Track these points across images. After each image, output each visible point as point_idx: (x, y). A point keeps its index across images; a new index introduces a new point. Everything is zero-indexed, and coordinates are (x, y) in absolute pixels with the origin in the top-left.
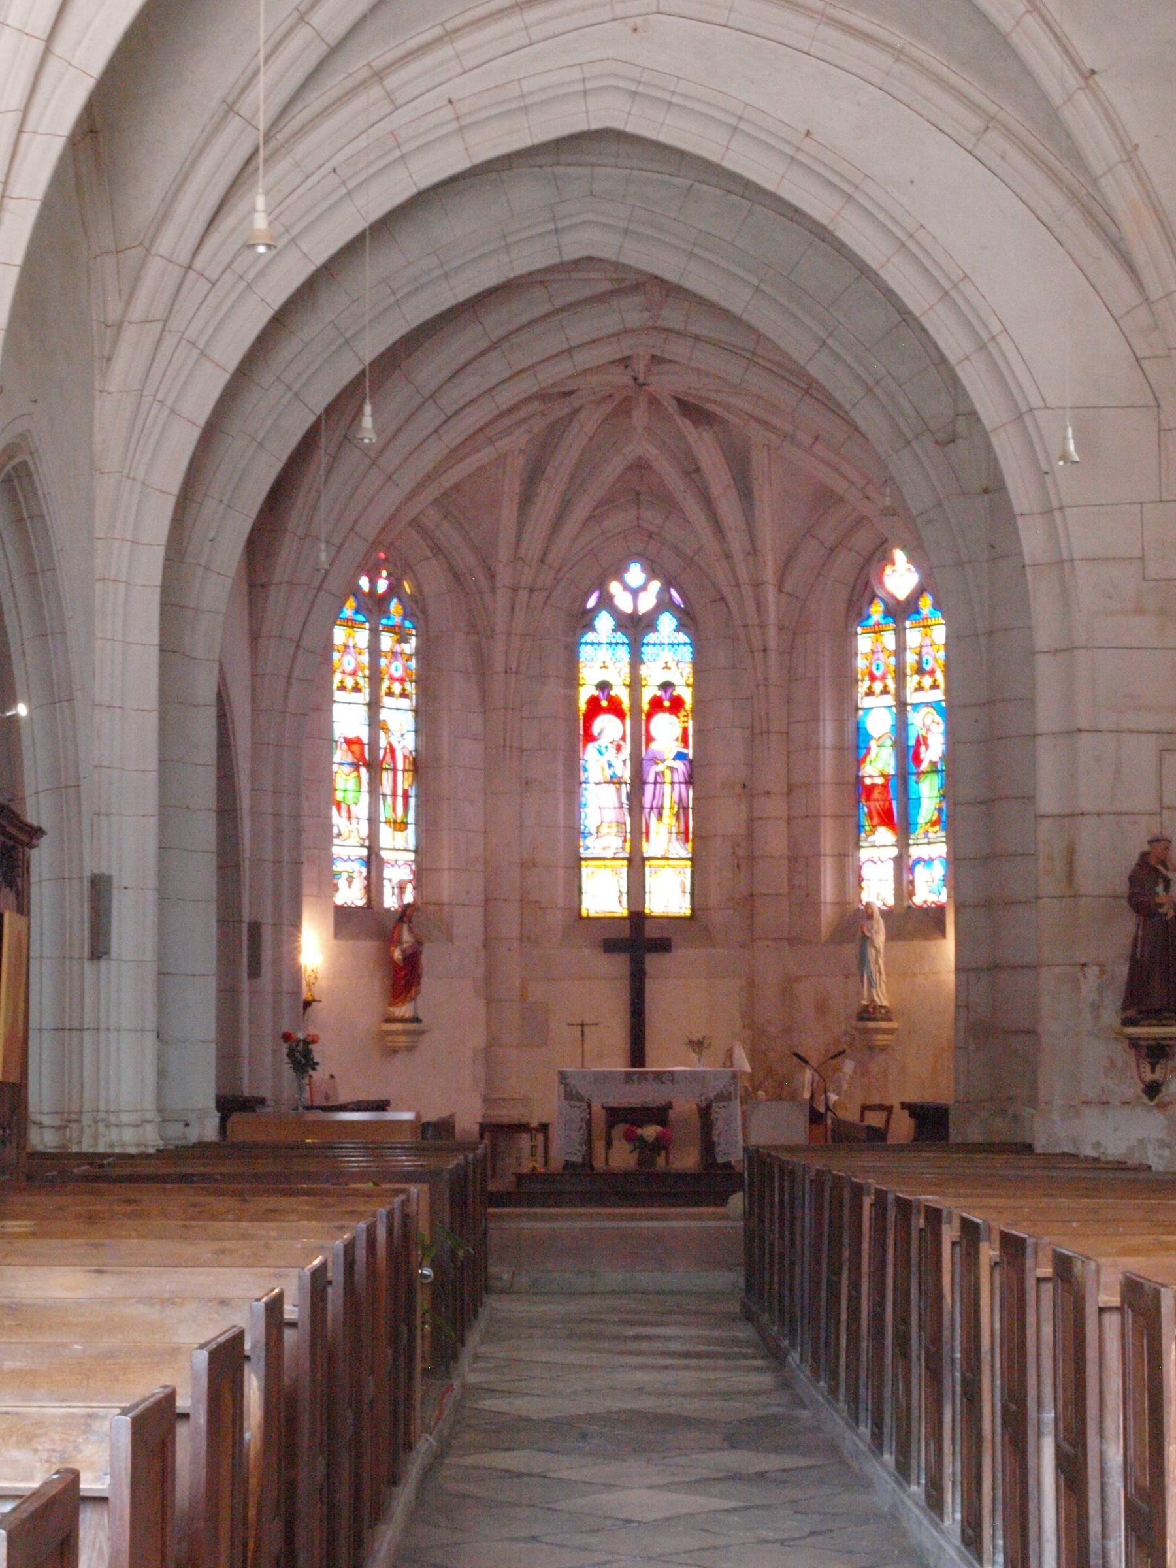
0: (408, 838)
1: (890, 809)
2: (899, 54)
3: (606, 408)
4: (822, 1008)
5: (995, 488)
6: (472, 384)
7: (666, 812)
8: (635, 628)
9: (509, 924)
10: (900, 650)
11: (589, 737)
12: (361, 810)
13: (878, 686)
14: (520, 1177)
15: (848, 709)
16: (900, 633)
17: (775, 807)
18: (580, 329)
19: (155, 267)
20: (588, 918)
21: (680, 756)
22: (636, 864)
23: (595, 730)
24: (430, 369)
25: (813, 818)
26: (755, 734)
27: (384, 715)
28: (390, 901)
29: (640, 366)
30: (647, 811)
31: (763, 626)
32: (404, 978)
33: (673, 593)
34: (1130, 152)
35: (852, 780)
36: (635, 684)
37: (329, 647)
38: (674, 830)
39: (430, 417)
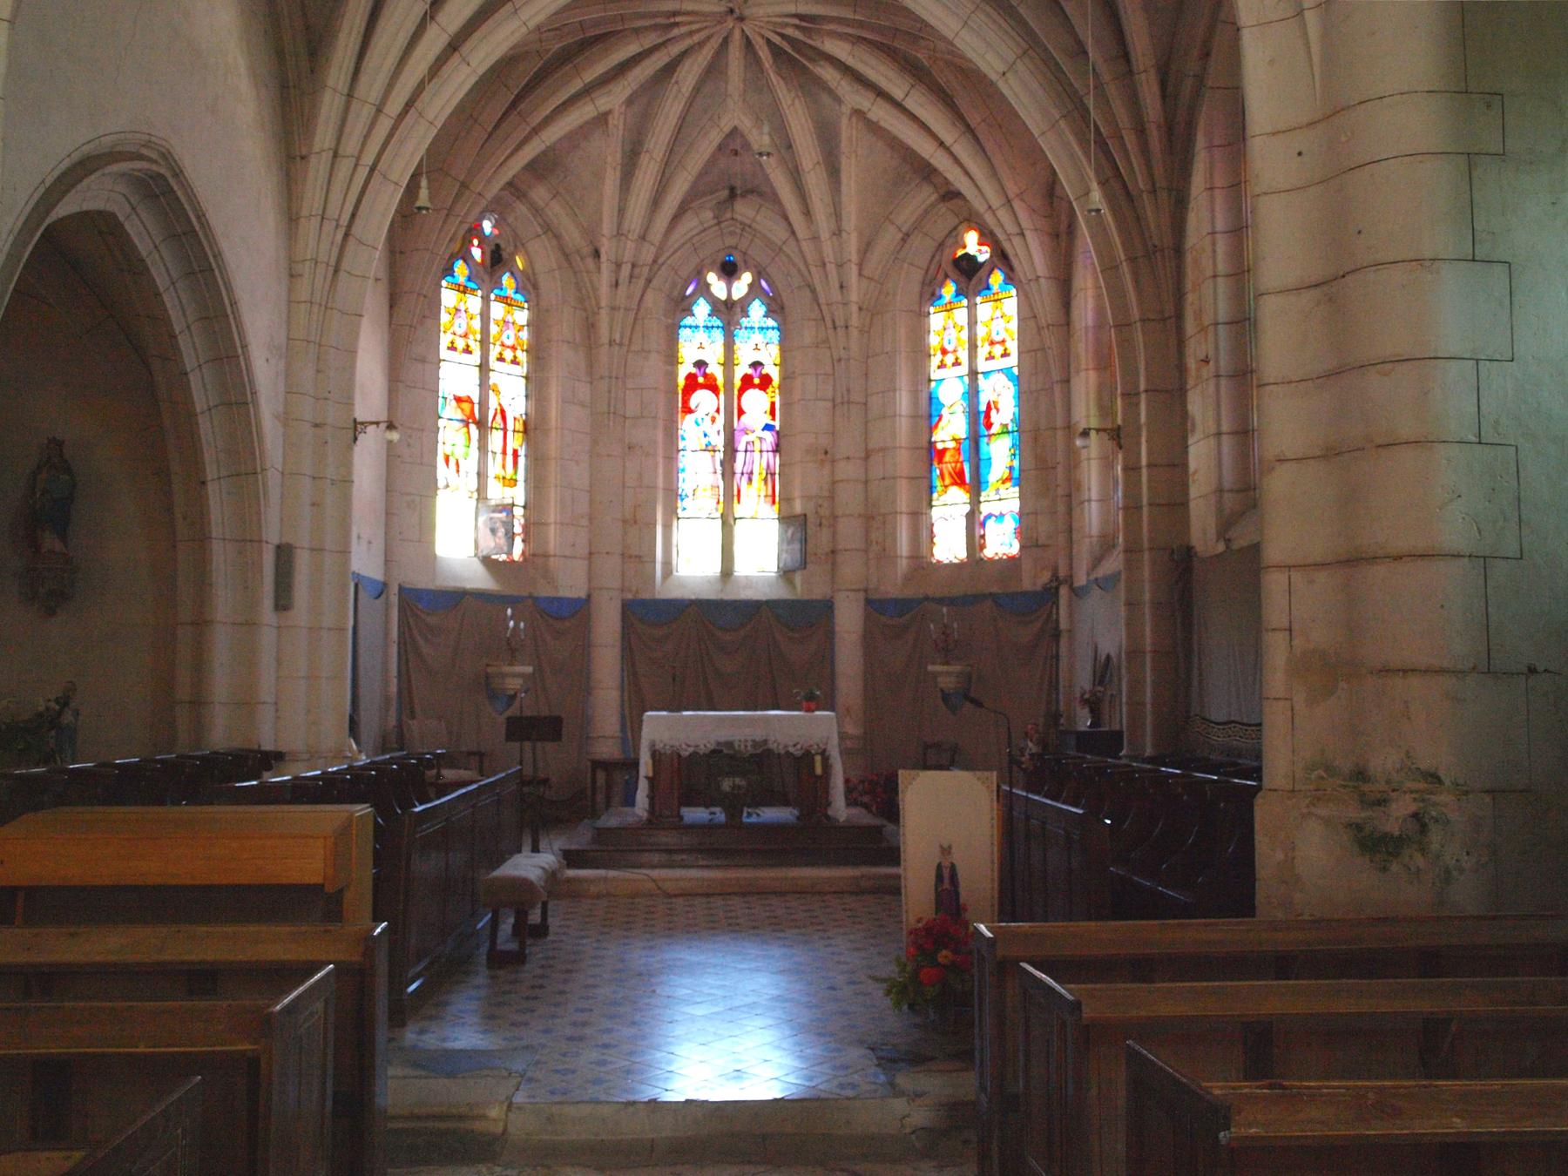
1: (961, 474)
7: (755, 477)
8: (729, 313)
10: (972, 322)
11: (688, 410)
12: (470, 465)
13: (949, 359)
16: (972, 308)
21: (768, 427)
23: (692, 404)
26: (837, 404)
27: (494, 378)
30: (738, 476)
33: (764, 283)
35: (925, 444)
36: (729, 363)
37: (433, 305)
38: (763, 493)
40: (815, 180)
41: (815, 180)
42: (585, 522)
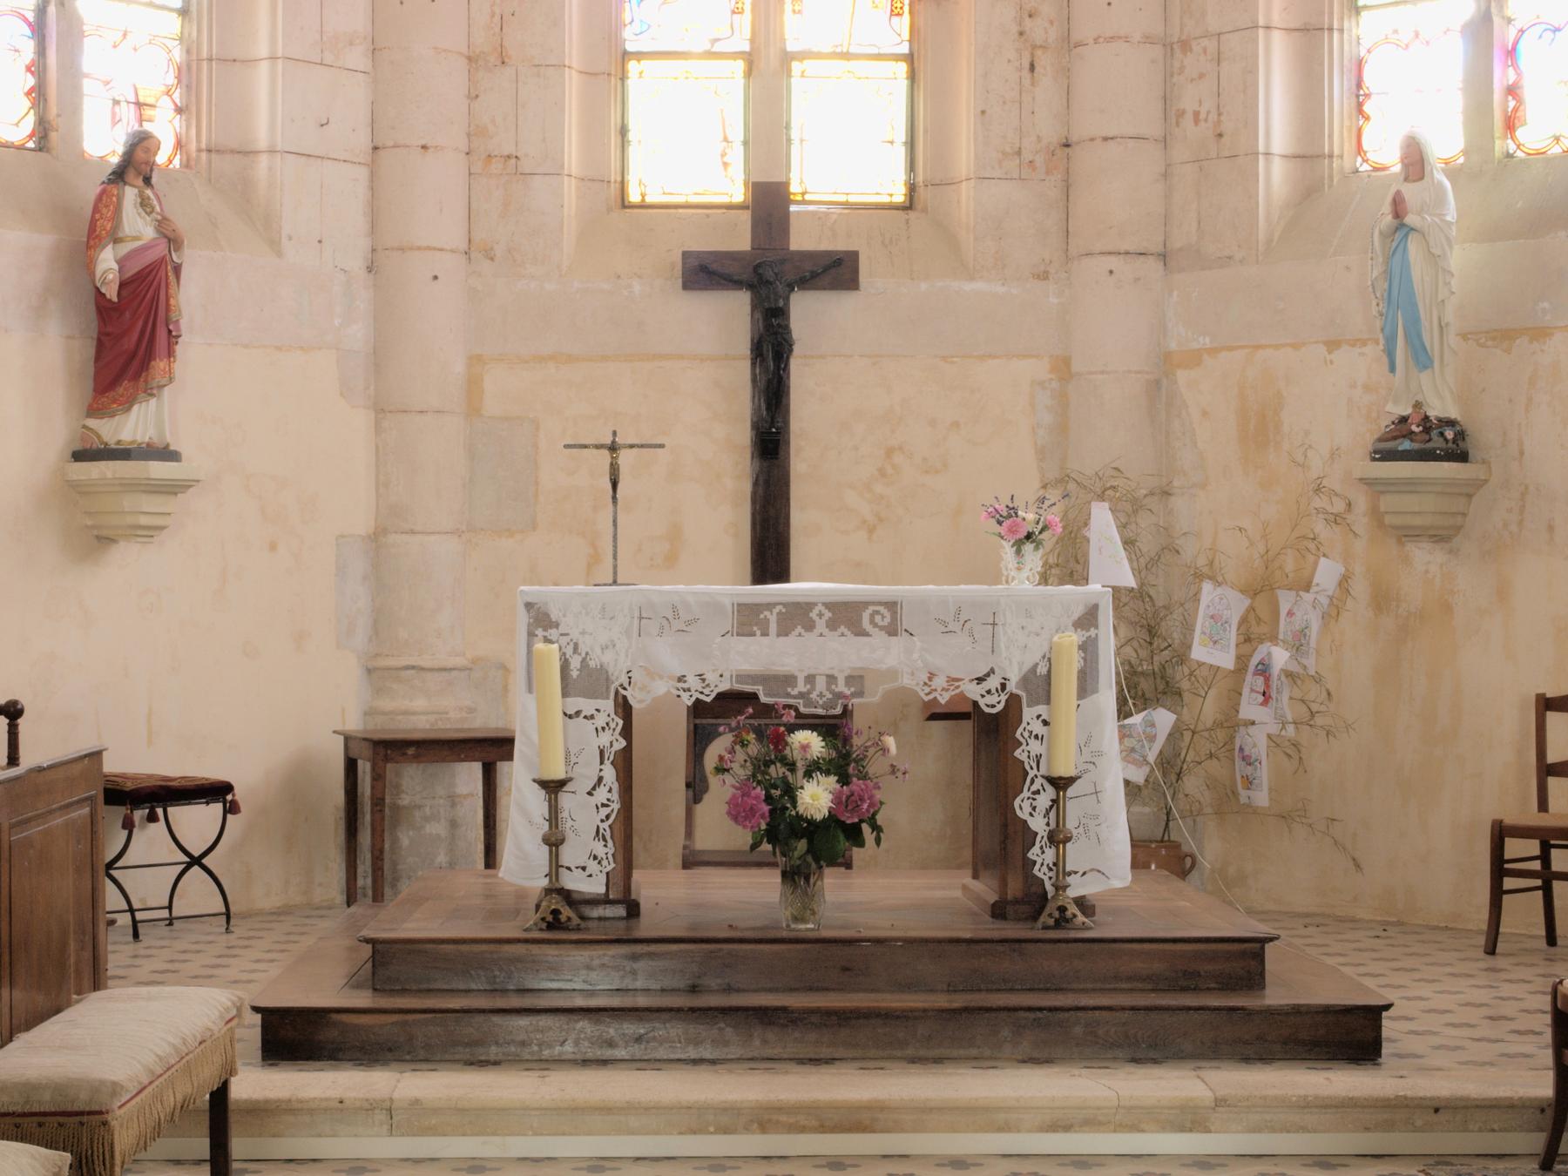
4: (1260, 427)
9: (436, 206)
20: (643, 206)
22: (767, 69)
42: (357, 57)
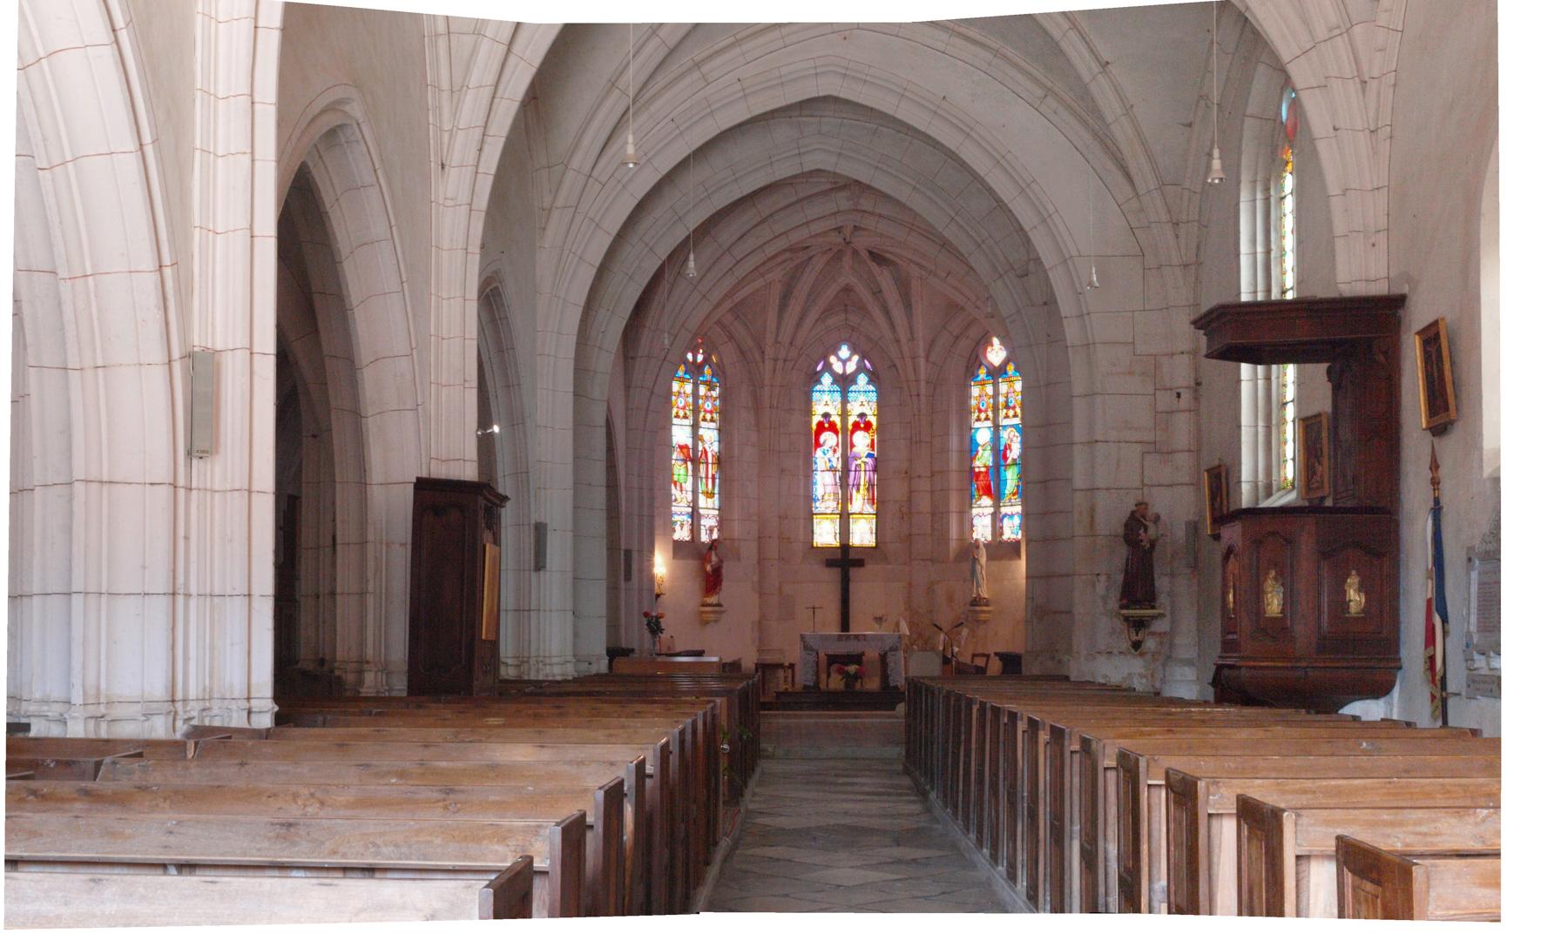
0: (715, 502)
2: (996, 53)
3: (826, 258)
4: (950, 599)
5: (1050, 302)
6: (750, 244)
8: (844, 382)
10: (996, 395)
11: (818, 445)
12: (688, 486)
13: (983, 416)
14: (779, 694)
15: (966, 431)
16: (996, 386)
17: (923, 485)
18: (814, 210)
19: (570, 175)
21: (869, 455)
22: (845, 517)
24: (727, 233)
25: (945, 491)
27: (701, 432)
28: (704, 538)
29: (847, 232)
31: (917, 381)
32: (712, 582)
34: (1128, 110)
36: (844, 414)
37: (670, 393)
39: (727, 262)
40: (898, 313)
41: (898, 313)
